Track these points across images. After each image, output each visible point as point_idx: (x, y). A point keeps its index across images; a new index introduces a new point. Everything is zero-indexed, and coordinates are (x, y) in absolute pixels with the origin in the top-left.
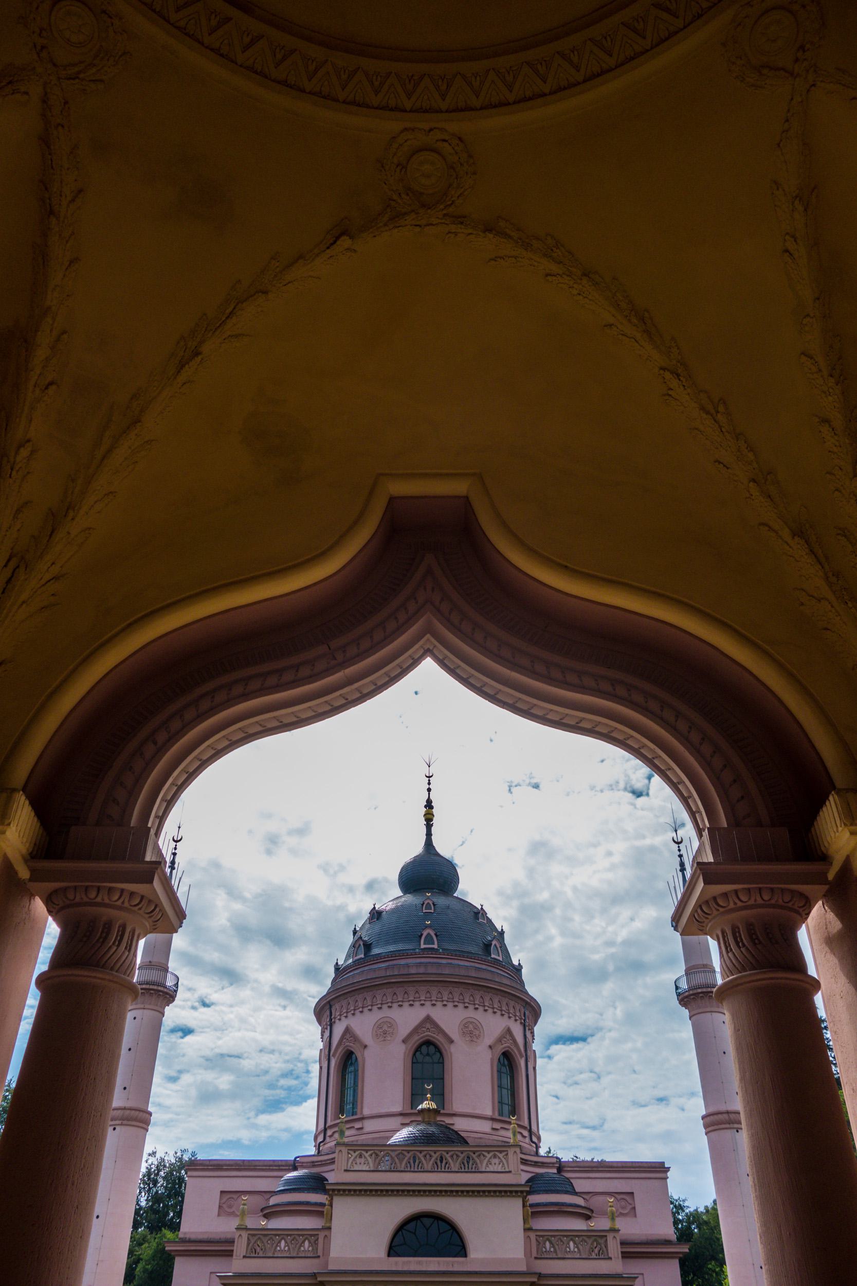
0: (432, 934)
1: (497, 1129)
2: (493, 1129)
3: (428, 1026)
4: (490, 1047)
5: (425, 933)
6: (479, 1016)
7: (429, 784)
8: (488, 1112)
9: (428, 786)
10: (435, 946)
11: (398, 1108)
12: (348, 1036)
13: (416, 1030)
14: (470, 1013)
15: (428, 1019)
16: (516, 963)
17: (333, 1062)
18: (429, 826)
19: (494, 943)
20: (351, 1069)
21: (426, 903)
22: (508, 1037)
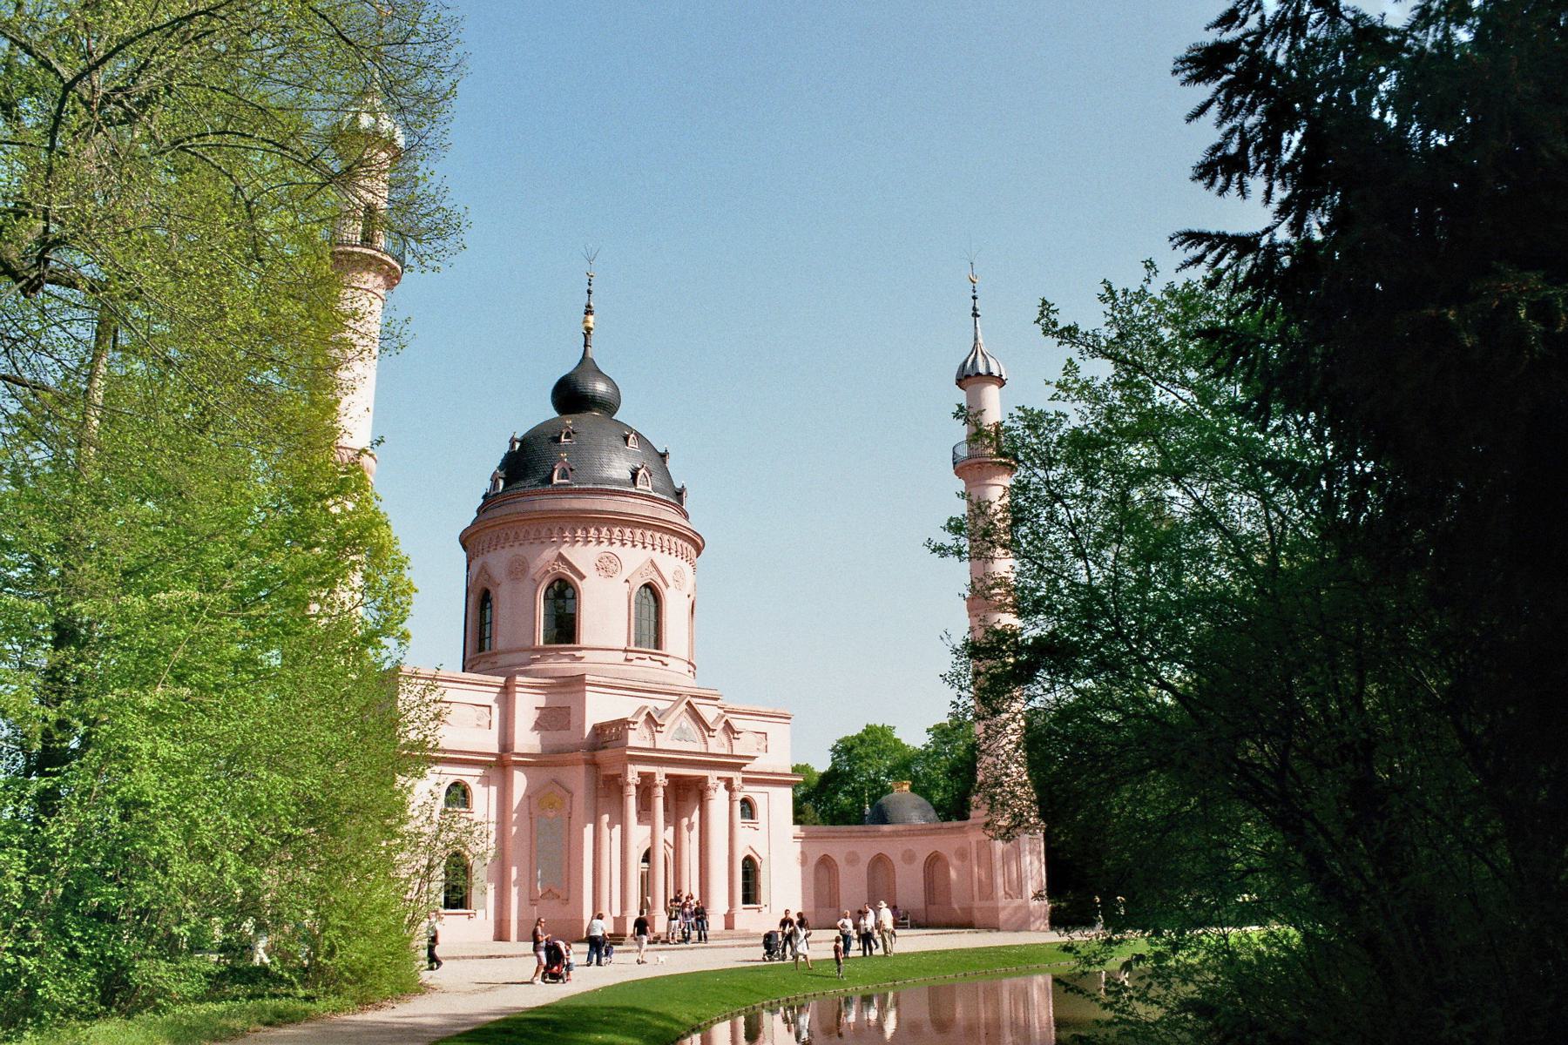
4: (627, 581)
6: (617, 547)
7: (590, 284)
8: (623, 645)
9: (588, 287)
11: (528, 643)
14: (605, 546)
15: (561, 557)
17: (472, 597)
19: (641, 472)
20: (488, 605)
21: (565, 431)
22: (651, 569)
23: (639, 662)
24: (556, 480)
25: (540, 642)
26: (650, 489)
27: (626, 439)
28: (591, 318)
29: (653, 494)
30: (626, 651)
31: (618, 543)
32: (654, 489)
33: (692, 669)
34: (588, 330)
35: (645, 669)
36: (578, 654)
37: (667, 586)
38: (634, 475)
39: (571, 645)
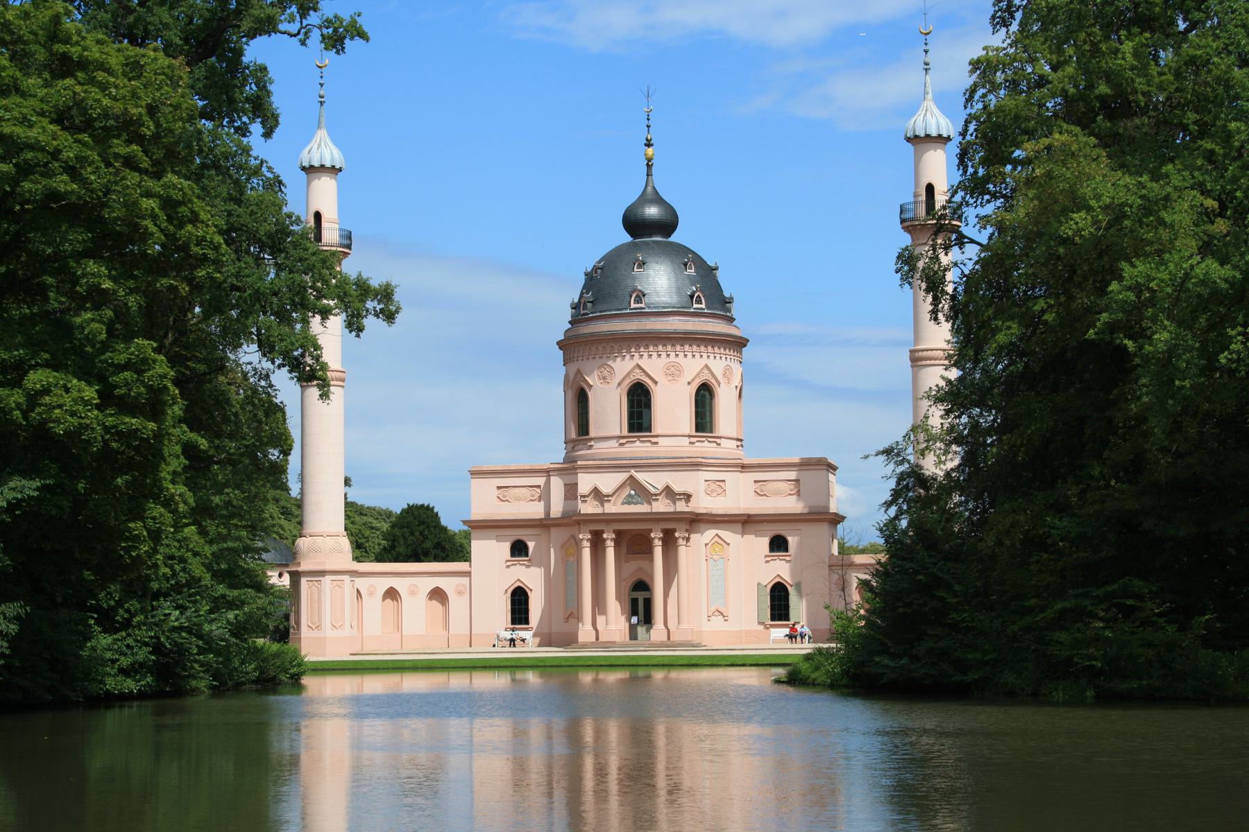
0: (641, 296)
1: (694, 443)
2: (690, 443)
3: (638, 371)
4: (689, 383)
5: (634, 296)
7: (648, 119)
8: (687, 432)
10: (643, 305)
11: (617, 433)
12: (579, 376)
13: (628, 375)
15: (638, 366)
16: (726, 294)
18: (649, 166)
22: (706, 371)
23: (697, 444)
24: (633, 306)
25: (625, 432)
26: (703, 306)
27: (685, 265)
28: (650, 151)
29: (706, 311)
30: (690, 436)
31: (681, 355)
32: (708, 307)
33: (739, 443)
34: (649, 160)
35: (705, 448)
36: (654, 440)
37: (719, 384)
38: (692, 297)
39: (648, 434)
